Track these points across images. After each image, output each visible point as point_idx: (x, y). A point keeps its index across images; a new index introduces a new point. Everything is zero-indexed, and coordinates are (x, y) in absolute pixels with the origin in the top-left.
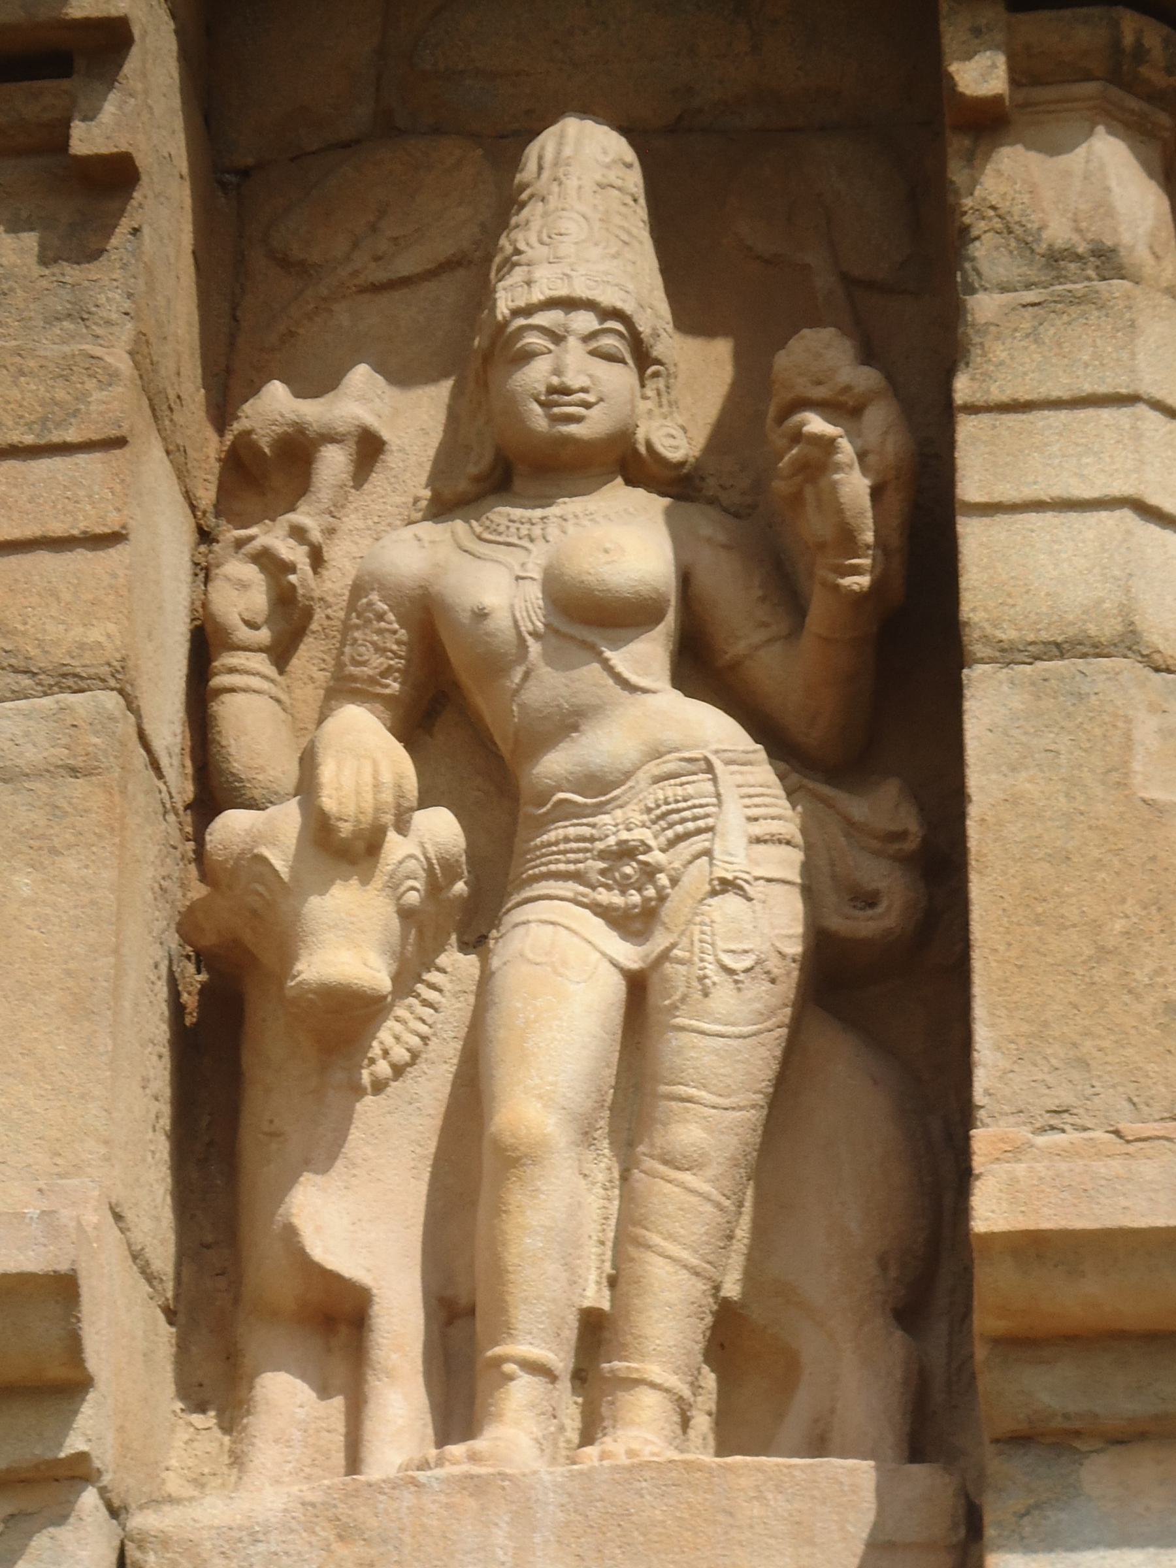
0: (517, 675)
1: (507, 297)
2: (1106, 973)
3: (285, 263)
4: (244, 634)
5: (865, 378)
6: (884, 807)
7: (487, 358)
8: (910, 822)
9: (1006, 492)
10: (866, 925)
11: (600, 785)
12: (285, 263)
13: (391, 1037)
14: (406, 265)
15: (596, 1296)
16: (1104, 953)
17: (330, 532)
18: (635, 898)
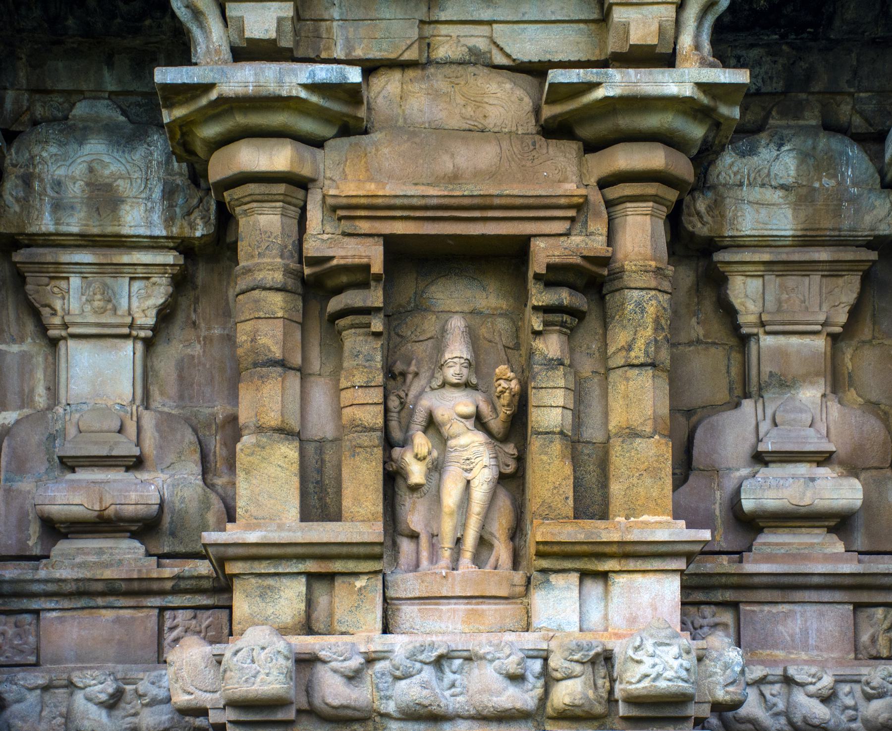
0: (449, 426)
1: (447, 356)
2: (555, 491)
3: (399, 335)
4: (393, 409)
5: (512, 375)
6: (511, 449)
7: (442, 365)
8: (515, 452)
9: (540, 404)
10: (509, 470)
11: (465, 447)
12: (399, 335)
13: (425, 489)
14: (421, 338)
15: (459, 535)
16: (555, 488)
17: (408, 390)
18: (468, 467)
